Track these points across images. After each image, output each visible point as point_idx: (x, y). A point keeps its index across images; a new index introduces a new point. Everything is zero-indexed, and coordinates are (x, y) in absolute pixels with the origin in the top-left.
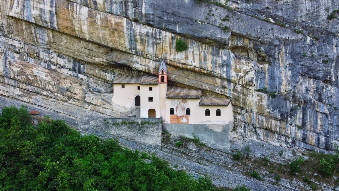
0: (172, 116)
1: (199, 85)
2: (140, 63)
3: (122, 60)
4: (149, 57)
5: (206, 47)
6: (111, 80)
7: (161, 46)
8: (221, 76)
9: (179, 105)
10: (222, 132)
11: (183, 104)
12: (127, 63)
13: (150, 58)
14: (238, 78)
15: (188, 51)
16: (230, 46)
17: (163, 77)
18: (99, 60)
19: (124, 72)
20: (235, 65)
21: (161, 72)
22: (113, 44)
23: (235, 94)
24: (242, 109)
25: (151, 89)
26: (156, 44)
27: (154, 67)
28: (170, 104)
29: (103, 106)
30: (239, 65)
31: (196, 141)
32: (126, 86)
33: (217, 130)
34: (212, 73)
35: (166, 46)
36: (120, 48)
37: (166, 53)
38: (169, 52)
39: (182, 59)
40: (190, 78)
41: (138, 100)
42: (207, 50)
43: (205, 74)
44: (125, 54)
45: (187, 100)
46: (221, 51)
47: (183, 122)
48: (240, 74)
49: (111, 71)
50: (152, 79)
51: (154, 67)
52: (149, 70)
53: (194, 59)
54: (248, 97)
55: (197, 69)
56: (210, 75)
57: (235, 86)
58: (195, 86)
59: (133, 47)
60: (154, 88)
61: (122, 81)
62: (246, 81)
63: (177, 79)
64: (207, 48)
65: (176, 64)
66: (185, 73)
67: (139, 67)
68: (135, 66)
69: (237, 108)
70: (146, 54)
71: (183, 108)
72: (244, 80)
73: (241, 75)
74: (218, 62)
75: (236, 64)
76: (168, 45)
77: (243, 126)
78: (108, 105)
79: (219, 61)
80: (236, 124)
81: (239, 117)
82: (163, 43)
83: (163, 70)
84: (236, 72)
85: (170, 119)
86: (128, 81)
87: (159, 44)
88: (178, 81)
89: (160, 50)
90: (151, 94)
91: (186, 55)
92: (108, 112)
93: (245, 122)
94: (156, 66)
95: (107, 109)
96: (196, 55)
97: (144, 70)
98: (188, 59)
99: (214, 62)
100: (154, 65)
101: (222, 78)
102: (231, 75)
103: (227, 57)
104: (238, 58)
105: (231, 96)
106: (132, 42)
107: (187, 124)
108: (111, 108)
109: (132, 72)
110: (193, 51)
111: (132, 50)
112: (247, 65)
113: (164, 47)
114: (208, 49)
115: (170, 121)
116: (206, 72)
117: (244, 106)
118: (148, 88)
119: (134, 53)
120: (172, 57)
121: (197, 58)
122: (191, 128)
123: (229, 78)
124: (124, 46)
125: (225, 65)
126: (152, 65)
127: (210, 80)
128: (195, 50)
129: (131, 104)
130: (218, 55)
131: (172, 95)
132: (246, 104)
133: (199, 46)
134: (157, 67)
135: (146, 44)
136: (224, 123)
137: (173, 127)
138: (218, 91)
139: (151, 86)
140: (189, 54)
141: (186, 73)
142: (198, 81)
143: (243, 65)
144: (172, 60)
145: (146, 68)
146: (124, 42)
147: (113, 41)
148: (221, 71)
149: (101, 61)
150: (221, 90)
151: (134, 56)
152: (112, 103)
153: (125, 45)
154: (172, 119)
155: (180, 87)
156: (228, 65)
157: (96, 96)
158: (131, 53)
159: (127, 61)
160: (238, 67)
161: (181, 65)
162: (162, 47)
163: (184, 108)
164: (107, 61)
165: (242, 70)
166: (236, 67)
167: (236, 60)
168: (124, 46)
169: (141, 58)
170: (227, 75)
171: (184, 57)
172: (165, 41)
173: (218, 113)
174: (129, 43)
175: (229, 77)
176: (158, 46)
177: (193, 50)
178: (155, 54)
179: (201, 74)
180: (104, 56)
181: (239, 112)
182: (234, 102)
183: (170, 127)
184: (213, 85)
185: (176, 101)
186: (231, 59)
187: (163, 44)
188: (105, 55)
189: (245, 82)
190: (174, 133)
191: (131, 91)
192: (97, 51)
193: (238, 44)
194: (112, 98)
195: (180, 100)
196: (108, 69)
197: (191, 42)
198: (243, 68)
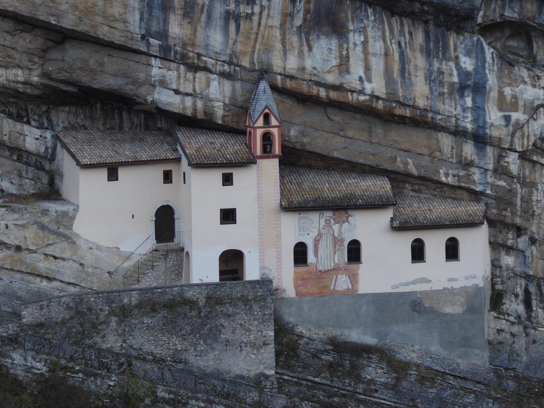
1: (383, 157)
2: (174, 87)
3: (108, 75)
4: (206, 62)
5: (402, 25)
6: (42, 150)
7: (255, 24)
8: (457, 126)
9: (323, 231)
10: (464, 312)
11: (336, 227)
12: (129, 89)
13: (210, 66)
14: (511, 128)
15: (348, 42)
16: (479, 20)
17: (267, 138)
18: (11, 78)
19: (92, 118)
20: (499, 87)
21: (261, 119)
22: (80, 20)
23: (502, 183)
24: (519, 231)
25: (228, 180)
26: (237, 18)
27: (227, 101)
28: (293, 229)
29: (49, 251)
30: (510, 85)
31: (383, 354)
32: (122, 172)
33: (449, 310)
34: (430, 115)
35: (270, 23)
36: (104, 32)
37: (268, 49)
38: (279, 46)
39: (329, 72)
40: (350, 134)
41: (165, 222)
42: (407, 36)
43: (402, 121)
44: (116, 53)
45: (350, 212)
46: (452, 39)
47: (338, 289)
48: (515, 116)
49: (40, 116)
50: (231, 147)
51: (227, 101)
52: (209, 113)
53: (367, 69)
54: (537, 190)
55: (380, 105)
56: (421, 122)
57: (500, 157)
58: (369, 163)
59: (155, 27)
60: (238, 175)
61: (107, 154)
62: (532, 139)
63: (306, 140)
64: (406, 29)
65: (304, 88)
66: (332, 117)
67: (170, 100)
68: (156, 96)
69: (504, 231)
70: (199, 55)
71: (337, 241)
72: (526, 134)
73: (517, 121)
74: (446, 79)
75: (503, 82)
76: (276, 21)
77: (519, 290)
78: (65, 245)
79: (451, 75)
80: (499, 287)
81: (508, 260)
82: (261, 13)
83: (267, 111)
84: (501, 109)
85: (296, 279)
86: (127, 152)
87: (249, 17)
88: (308, 148)
89: (248, 38)
90: (228, 197)
91: (341, 56)
92: (67, 271)
93: (527, 277)
94: (233, 98)
95: (62, 263)
96: (375, 55)
97: (189, 113)
98: (348, 72)
99: (433, 79)
100: (228, 93)
101: (458, 133)
102: (488, 120)
103: (474, 61)
104: (507, 61)
105: (488, 192)
106: (150, 13)
108: (75, 258)
109: (121, 119)
110: (365, 43)
111: (151, 40)
112: (534, 86)
113: (262, 28)
114: (411, 33)
115: (296, 287)
116: (408, 113)
117: (525, 224)
118: (217, 176)
119: (154, 50)
120: (292, 63)
121: (378, 64)
122: (364, 308)
123: (481, 132)
124: (120, 25)
125: (468, 86)
126: (218, 93)
127: (418, 139)
128: (370, 40)
129: (139, 240)
130: (444, 53)
131: (296, 199)
132: (533, 215)
133: (382, 23)
134: (240, 99)
135: (204, 18)
136: (470, 283)
137: (306, 307)
138: (447, 176)
139: (227, 171)
140: (351, 53)
141: (338, 117)
142: (380, 144)
143: (522, 86)
144: (294, 73)
145: (200, 104)
146: (122, 11)
147: (82, 7)
148: (459, 108)
149: (21, 79)
150: (455, 172)
151: (153, 61)
152: (74, 239)
153: (125, 22)
154: (299, 281)
155: (310, 167)
156: (479, 89)
157: (16, 216)
158: (143, 49)
159: (126, 80)
160: (508, 91)
161: (323, 93)
162: (255, 30)
163: (342, 240)
164: (44, 81)
165: (521, 103)
166: (501, 93)
167: (500, 70)
168: (120, 25)
169: (178, 70)
170: (475, 120)
171: (335, 62)
172: (269, 8)
173: (452, 251)
174: (142, 14)
175: (484, 128)
176: (242, 23)
177: (366, 38)
178: (228, 51)
179: (385, 121)
180: (30, 61)
181: (510, 242)
182: (494, 211)
183: (293, 309)
184: (430, 155)
185: (314, 217)
186: (487, 65)
187: (260, 18)
188: (36, 60)
189: (531, 143)
190: (311, 328)
191: (140, 190)
192: (7, 43)
193: (506, 14)
194: (73, 218)
195: (328, 214)
196: (30, 107)
197: (354, 12)
198: (526, 96)
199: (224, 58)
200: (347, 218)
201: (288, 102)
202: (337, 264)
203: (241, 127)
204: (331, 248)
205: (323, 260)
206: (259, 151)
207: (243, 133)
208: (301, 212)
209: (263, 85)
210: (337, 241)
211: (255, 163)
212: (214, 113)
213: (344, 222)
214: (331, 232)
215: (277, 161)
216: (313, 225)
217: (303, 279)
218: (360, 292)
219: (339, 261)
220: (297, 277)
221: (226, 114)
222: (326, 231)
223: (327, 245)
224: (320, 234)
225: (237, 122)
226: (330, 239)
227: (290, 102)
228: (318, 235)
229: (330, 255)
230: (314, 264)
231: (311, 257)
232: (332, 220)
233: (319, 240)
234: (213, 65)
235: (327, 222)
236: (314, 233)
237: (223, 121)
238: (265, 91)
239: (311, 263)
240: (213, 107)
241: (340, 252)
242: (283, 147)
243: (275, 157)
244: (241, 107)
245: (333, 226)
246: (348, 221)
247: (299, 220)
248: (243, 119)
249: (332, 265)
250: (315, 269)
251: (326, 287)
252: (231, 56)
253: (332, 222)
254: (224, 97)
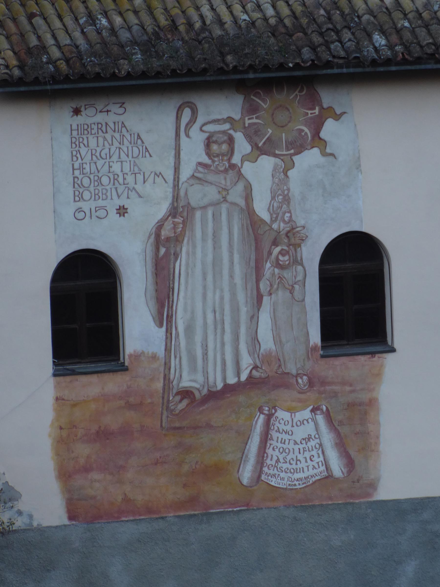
0: (94, 386)
9: (197, 195)
11: (261, 172)
45: (328, 97)
47: (279, 479)
71: (267, 243)
107: (346, 501)
115: (65, 475)
163: (293, 238)
195: (221, 109)
200: (317, 125)
202: (268, 358)
204: (238, 280)
205: (198, 338)
210: (266, 245)
213: (299, 146)
214: (236, 195)
216: (147, 164)
218: (384, 493)
219: (277, 340)
220: (73, 426)
222: (212, 193)
223: (217, 262)
224: (180, 211)
226: (232, 231)
228: (173, 212)
229: (235, 310)
230: (154, 357)
231: (138, 328)
232: (239, 137)
233: (178, 239)
235: (218, 147)
236: (152, 206)
239: (137, 357)
241: (281, 295)
245: (247, 169)
246: (317, 140)
247: (75, 143)
249: (247, 361)
250: (159, 385)
251: (218, 471)
253: (242, 146)
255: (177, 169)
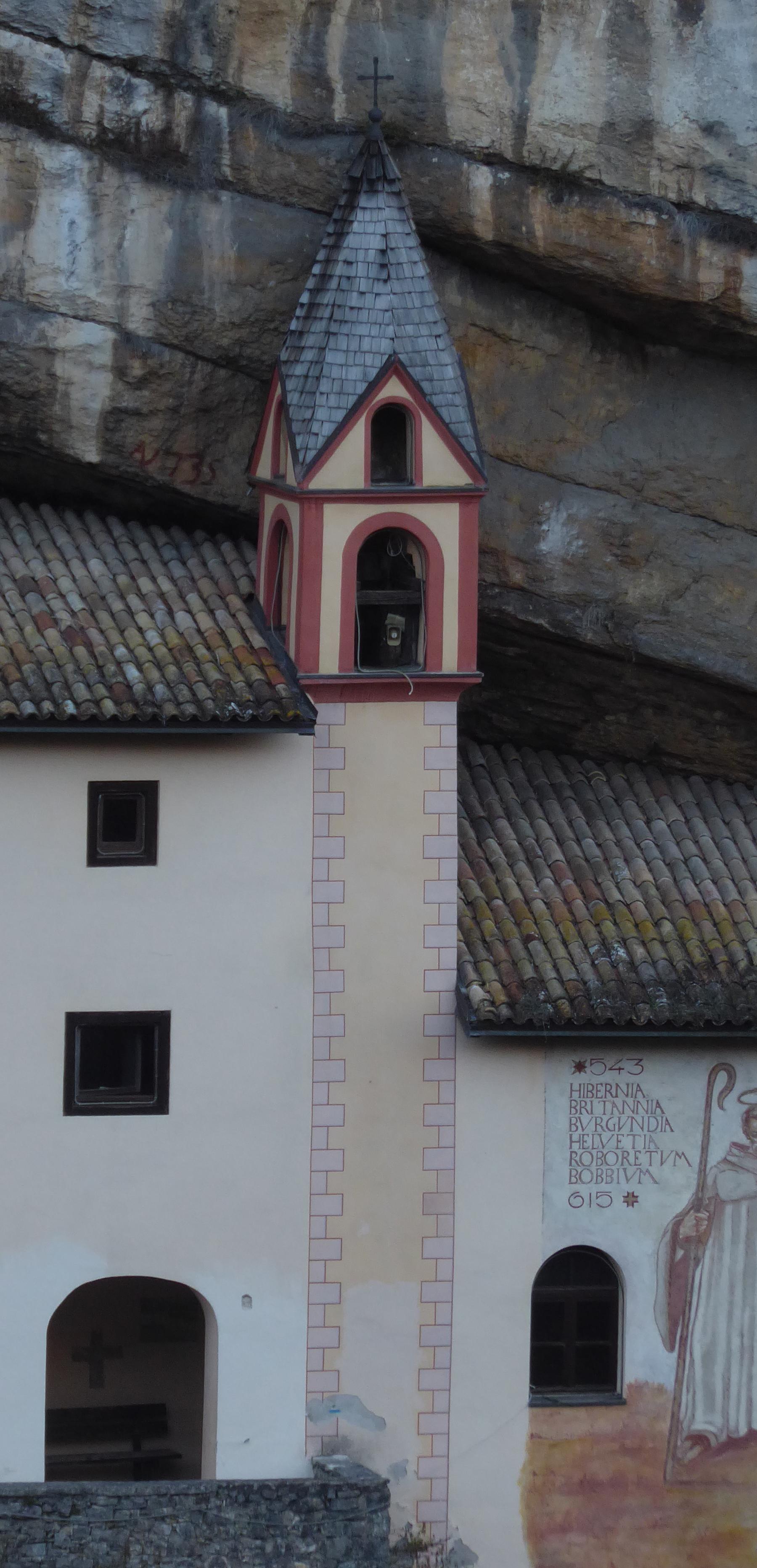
13: (37, 89)
17: (388, 566)
21: (356, 443)
25: (123, 828)
27: (139, 320)
28: (535, 1162)
50: (150, 614)
51: (139, 320)
60: (192, 797)
63: (640, 589)
65: (643, 252)
85: (538, 1488)
88: (653, 640)
90: (123, 941)
94: (180, 296)
131: (563, 966)
134: (223, 308)
139: (123, 768)
144: (578, 152)
155: (659, 765)
199: (131, 42)
201: (537, 342)
203: (225, 487)
206: (330, 649)
207: (234, 526)
208: (585, 1056)
209: (378, 225)
211: (305, 724)
212: (51, 393)
215: (444, 715)
216: (666, 1141)
217: (587, 1486)
221: (129, 401)
225: (199, 456)
227: (549, 341)
228: (697, 1205)
230: (660, 1390)
231: (642, 1350)
233: (700, 1240)
234: (58, 83)
236: (670, 1195)
237: (108, 445)
238: (385, 262)
239: (638, 1388)
240: (51, 352)
242: (492, 631)
243: (433, 688)
244: (227, 361)
247: (576, 1108)
248: (239, 439)
250: (664, 1426)
252: (177, 31)
254: (123, 291)
255: (705, 1149)
